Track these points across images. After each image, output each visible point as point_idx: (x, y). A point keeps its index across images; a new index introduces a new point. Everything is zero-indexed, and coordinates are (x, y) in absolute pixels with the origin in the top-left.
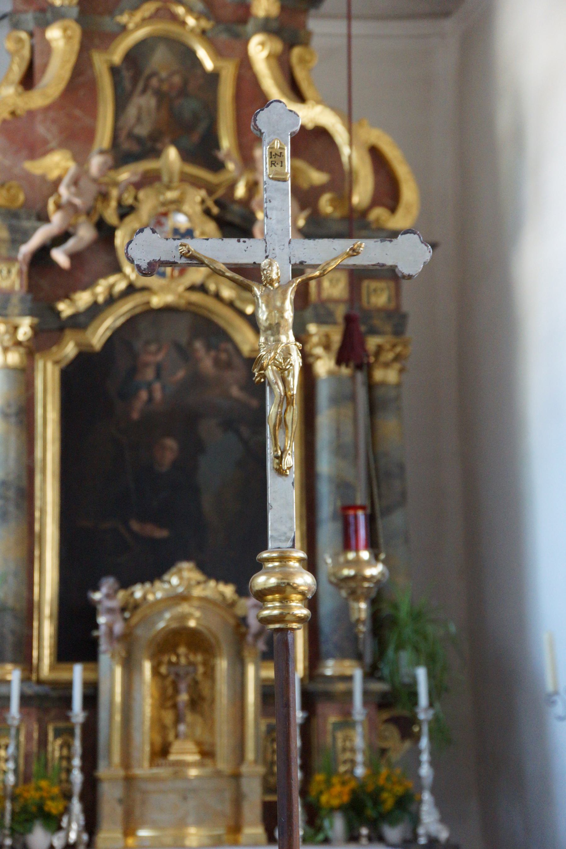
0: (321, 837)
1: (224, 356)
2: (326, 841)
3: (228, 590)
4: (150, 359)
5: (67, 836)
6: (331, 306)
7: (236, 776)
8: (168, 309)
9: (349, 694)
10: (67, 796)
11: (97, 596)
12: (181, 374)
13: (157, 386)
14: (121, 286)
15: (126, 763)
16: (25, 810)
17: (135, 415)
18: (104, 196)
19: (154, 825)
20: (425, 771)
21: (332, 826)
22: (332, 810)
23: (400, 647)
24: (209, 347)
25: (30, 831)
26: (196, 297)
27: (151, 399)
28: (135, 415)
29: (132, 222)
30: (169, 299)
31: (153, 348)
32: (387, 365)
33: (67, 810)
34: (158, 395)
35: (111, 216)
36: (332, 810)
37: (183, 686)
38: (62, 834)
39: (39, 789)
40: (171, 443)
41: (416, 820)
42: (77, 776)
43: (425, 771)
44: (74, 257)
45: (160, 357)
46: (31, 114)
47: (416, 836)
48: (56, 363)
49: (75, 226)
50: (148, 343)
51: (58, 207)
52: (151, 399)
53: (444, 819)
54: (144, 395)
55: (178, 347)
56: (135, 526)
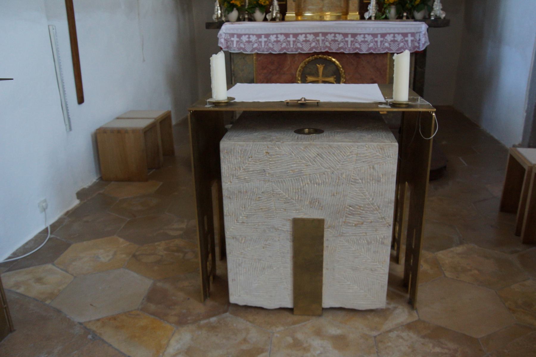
0: (384, 16)
2: (386, 19)
5: (272, 15)
19: (309, 10)
21: (389, 12)
22: (390, 4)
25: (254, 12)
36: (390, 4)
38: (270, 14)
41: (431, 9)
47: (430, 16)
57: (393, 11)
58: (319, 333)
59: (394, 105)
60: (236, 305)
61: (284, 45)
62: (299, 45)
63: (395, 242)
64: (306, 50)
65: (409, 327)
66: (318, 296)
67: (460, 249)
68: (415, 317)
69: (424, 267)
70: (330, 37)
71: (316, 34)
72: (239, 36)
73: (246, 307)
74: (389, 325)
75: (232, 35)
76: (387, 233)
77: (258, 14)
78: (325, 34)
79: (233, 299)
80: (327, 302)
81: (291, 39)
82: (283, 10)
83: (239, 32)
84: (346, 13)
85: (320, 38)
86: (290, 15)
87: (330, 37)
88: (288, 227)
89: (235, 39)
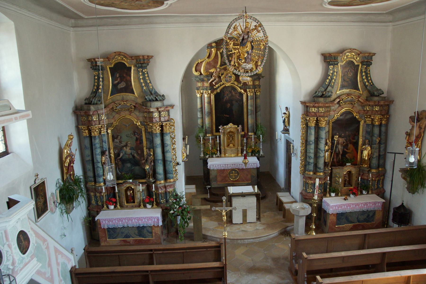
1: (236, 92)
3: (236, 126)
4: (226, 93)
6: (250, 86)
7: (238, 148)
8: (228, 86)
9: (252, 137)
10: (217, 151)
11: (220, 127)
12: (230, 95)
13: (227, 97)
14: (222, 84)
15: (224, 147)
16: (212, 153)
17: (224, 101)
18: (219, 73)
20: (261, 147)
22: (249, 152)
23: (259, 131)
24: (234, 91)
26: (232, 85)
27: (226, 98)
28: (224, 101)
29: (223, 76)
30: (228, 85)
31: (226, 92)
32: (258, 92)
33: (217, 152)
34: (227, 98)
35: (220, 75)
37: (231, 138)
39: (214, 151)
40: (229, 104)
41: (260, 152)
42: (218, 149)
43: (261, 147)
44: (215, 83)
45: (227, 93)
46: (210, 62)
48: (214, 94)
49: (216, 78)
50: (226, 91)
51: (213, 76)
52: (226, 98)
53: (263, 153)
54: (225, 98)
55: (229, 91)
56: (225, 115)
57: (250, 154)
58: (247, 226)
59: (255, 193)
60: (234, 224)
61: (225, 167)
62: (228, 167)
63: (257, 212)
64: (230, 168)
65: (260, 224)
66: (246, 221)
67: (268, 213)
68: (261, 223)
69: (261, 216)
70: (236, 165)
71: (233, 164)
72: (213, 165)
73: (235, 224)
74: (257, 224)
75: (211, 165)
76: (256, 210)
77: (214, 156)
78: (235, 164)
79: (233, 223)
80: (248, 221)
81: (226, 166)
82: (220, 153)
83: (213, 164)
84: (238, 154)
85: (234, 165)
86: (223, 155)
87: (236, 165)
88: (242, 210)
89: (212, 166)
